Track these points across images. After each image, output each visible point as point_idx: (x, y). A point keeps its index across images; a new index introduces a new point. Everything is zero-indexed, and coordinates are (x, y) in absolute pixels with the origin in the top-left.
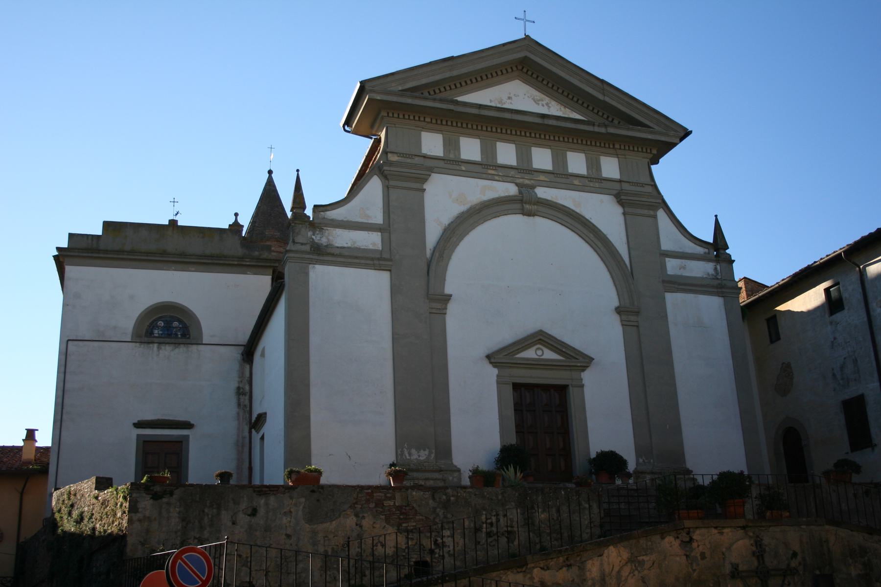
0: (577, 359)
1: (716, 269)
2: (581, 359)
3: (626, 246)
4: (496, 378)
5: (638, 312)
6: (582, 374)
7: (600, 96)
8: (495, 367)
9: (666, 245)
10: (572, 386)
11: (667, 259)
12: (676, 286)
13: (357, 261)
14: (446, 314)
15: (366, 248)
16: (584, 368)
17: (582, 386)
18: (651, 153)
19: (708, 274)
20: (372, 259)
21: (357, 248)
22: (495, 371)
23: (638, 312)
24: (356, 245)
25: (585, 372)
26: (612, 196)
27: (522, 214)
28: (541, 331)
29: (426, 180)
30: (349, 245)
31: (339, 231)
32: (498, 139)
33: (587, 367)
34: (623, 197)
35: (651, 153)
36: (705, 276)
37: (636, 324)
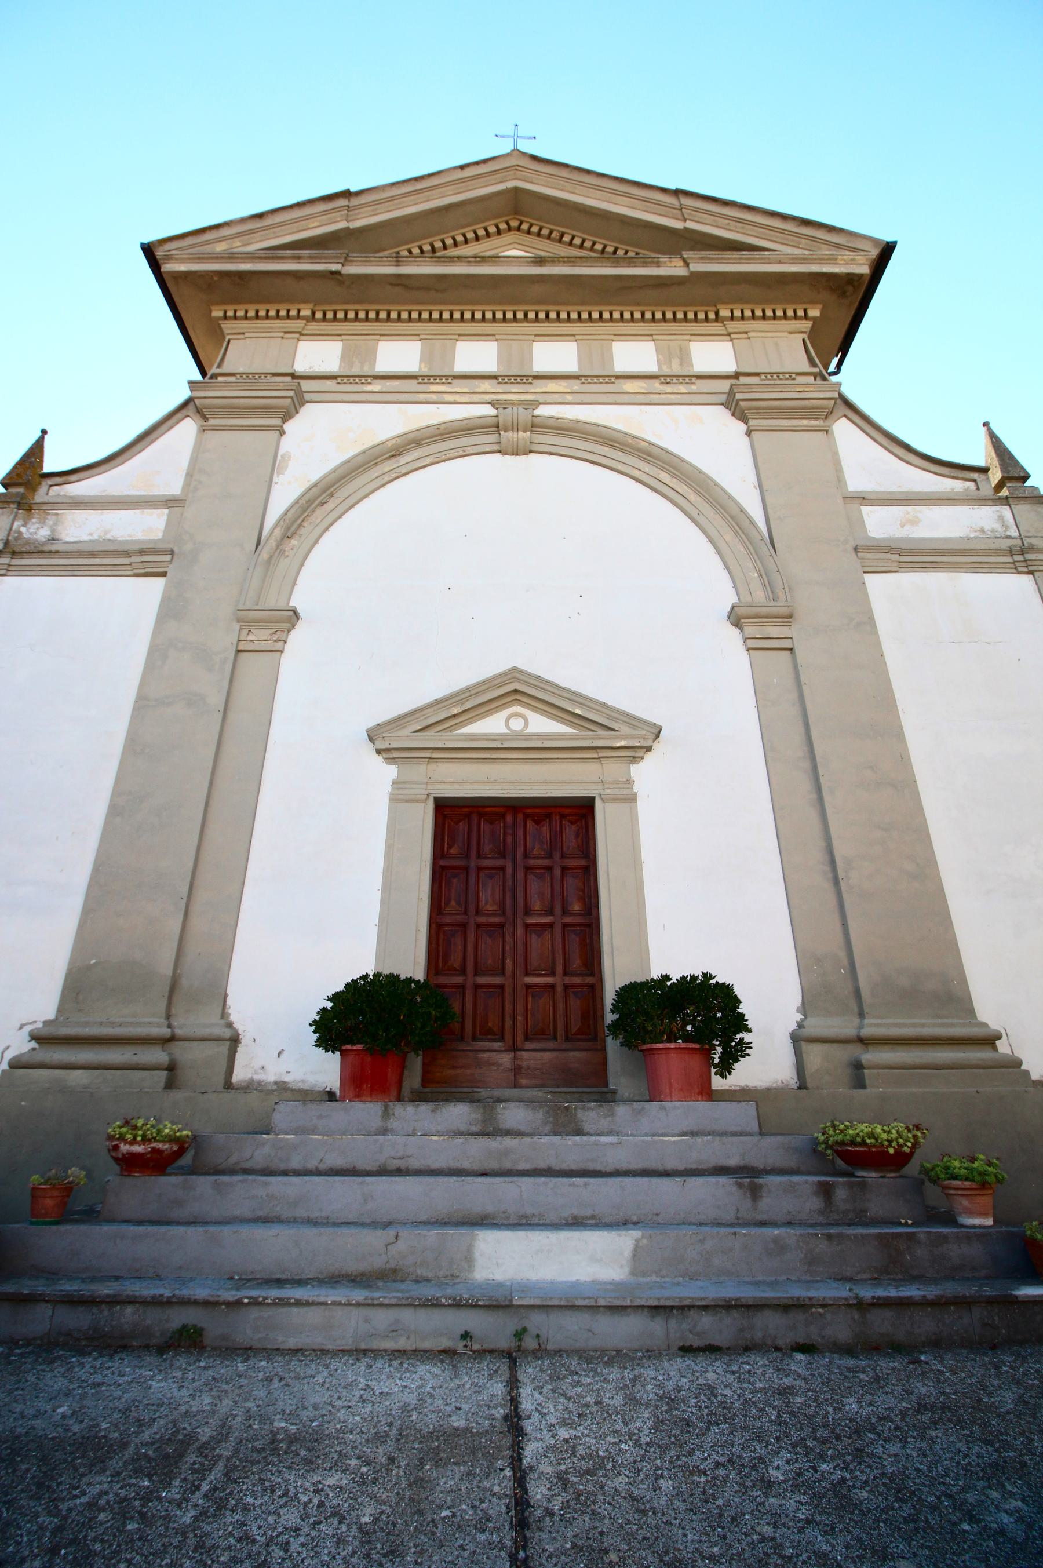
0: (614, 730)
1: (1001, 518)
2: (625, 729)
3: (756, 494)
4: (390, 789)
5: (790, 616)
6: (634, 769)
7: (678, 225)
8: (390, 760)
9: (855, 484)
10: (603, 800)
11: (865, 509)
12: (896, 557)
13: (97, 561)
14: (282, 652)
15: (128, 539)
16: (636, 753)
17: (632, 799)
18: (806, 317)
19: (982, 530)
20: (128, 554)
21: (109, 540)
22: (392, 771)
23: (790, 616)
24: (108, 536)
25: (642, 764)
26: (722, 407)
27: (500, 452)
28: (514, 669)
29: (287, 417)
30: (95, 537)
31: (80, 515)
32: (460, 335)
33: (649, 749)
34: (738, 396)
35: (806, 317)
36: (972, 535)
37: (787, 644)
